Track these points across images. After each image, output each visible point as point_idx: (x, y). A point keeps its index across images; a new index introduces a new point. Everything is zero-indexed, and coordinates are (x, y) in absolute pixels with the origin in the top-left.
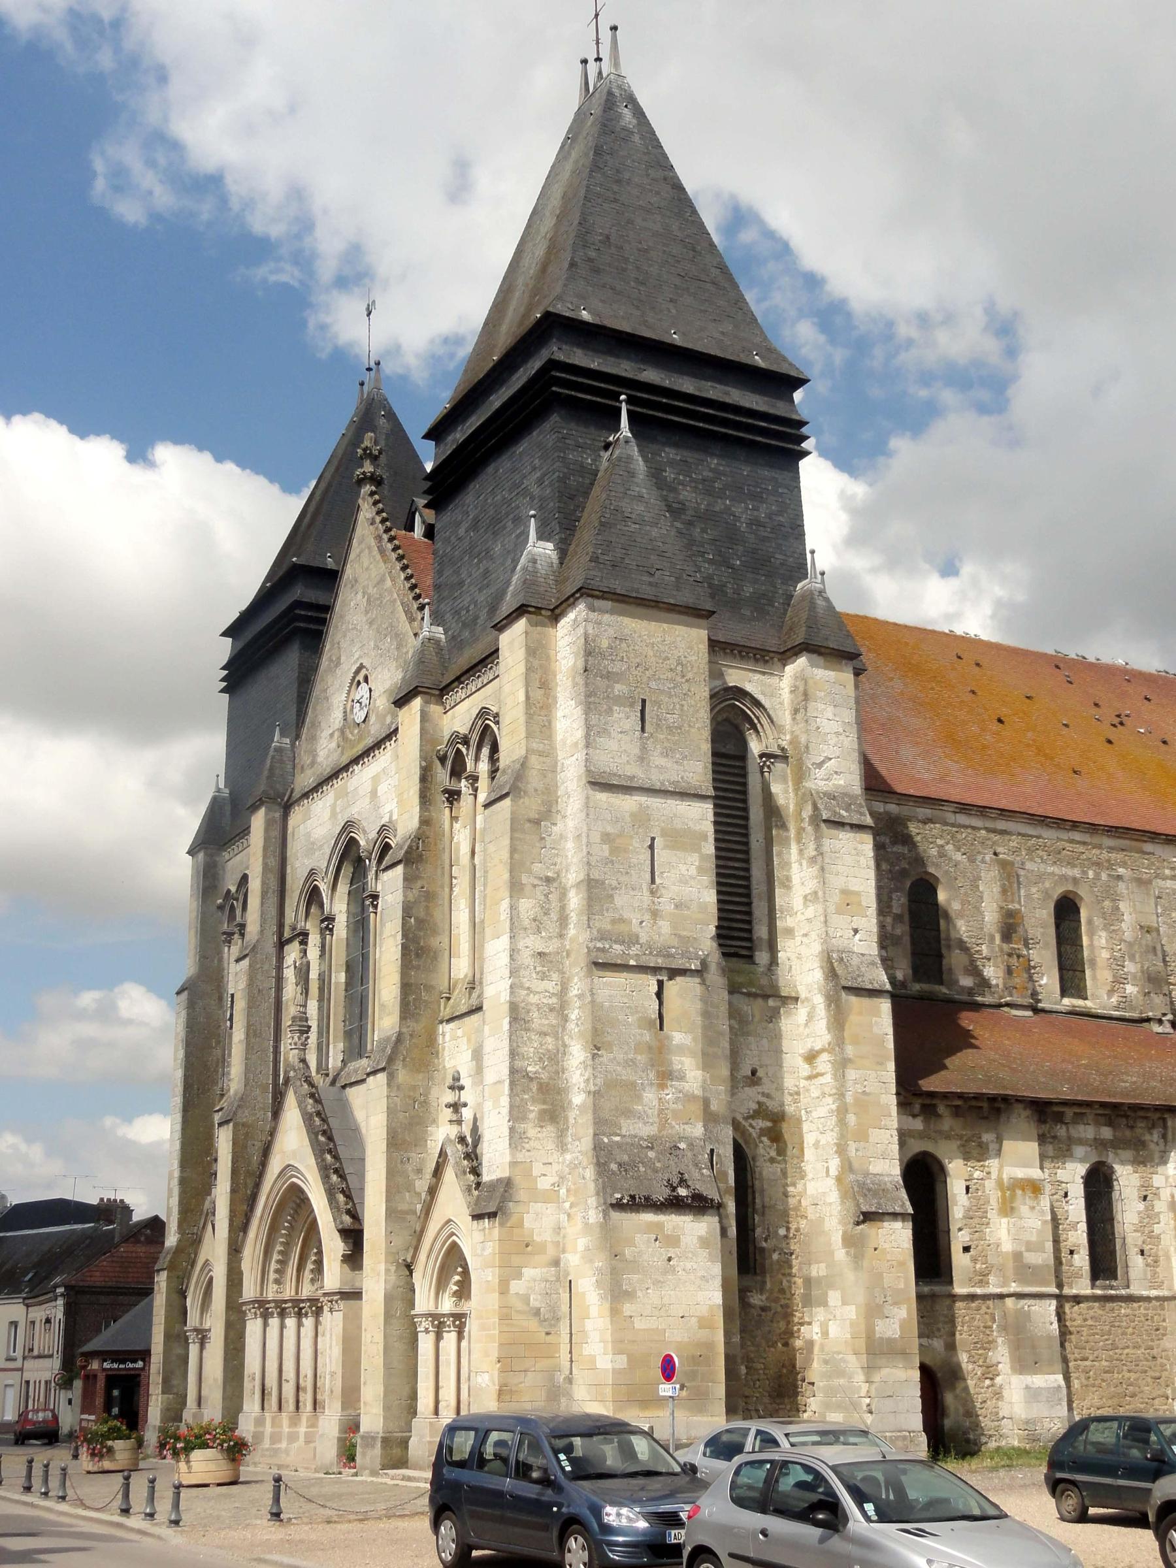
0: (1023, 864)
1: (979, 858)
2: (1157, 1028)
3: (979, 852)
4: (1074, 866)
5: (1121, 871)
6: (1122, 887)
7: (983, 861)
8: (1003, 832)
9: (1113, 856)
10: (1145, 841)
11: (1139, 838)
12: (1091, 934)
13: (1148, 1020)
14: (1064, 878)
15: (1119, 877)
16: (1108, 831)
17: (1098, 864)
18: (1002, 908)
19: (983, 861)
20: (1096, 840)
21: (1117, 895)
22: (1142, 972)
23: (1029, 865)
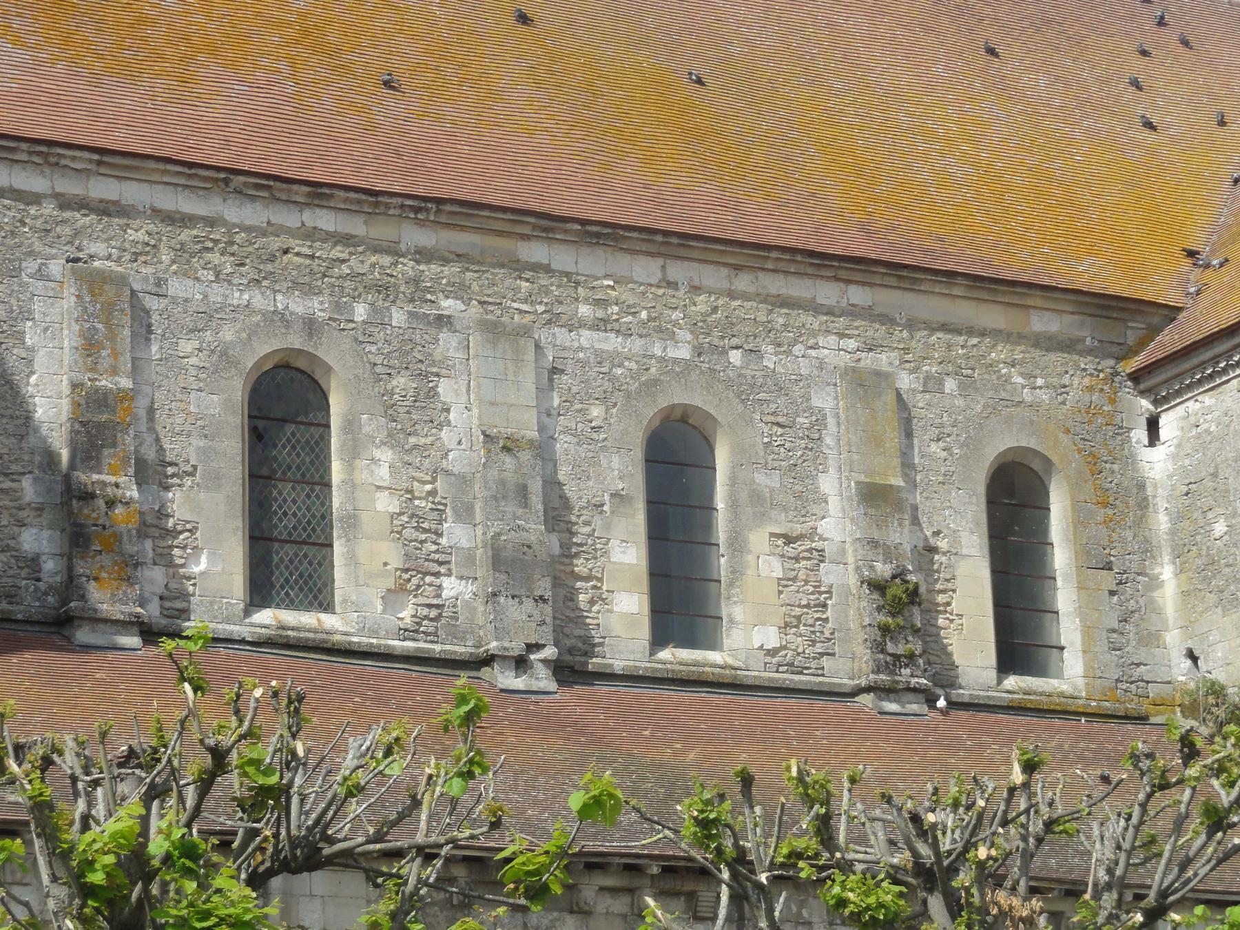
0: (159, 282)
1: (31, 266)
2: (508, 679)
3: (31, 254)
4: (309, 290)
5: (449, 305)
6: (447, 343)
7: (41, 275)
8: (106, 209)
9: (431, 270)
10: (525, 237)
11: (506, 227)
12: (353, 452)
13: (488, 660)
14: (282, 319)
15: (443, 321)
16: (417, 210)
17: (382, 289)
18: (75, 386)
19: (41, 275)
20: (382, 231)
21: (433, 363)
22: (485, 546)
23: (177, 287)
